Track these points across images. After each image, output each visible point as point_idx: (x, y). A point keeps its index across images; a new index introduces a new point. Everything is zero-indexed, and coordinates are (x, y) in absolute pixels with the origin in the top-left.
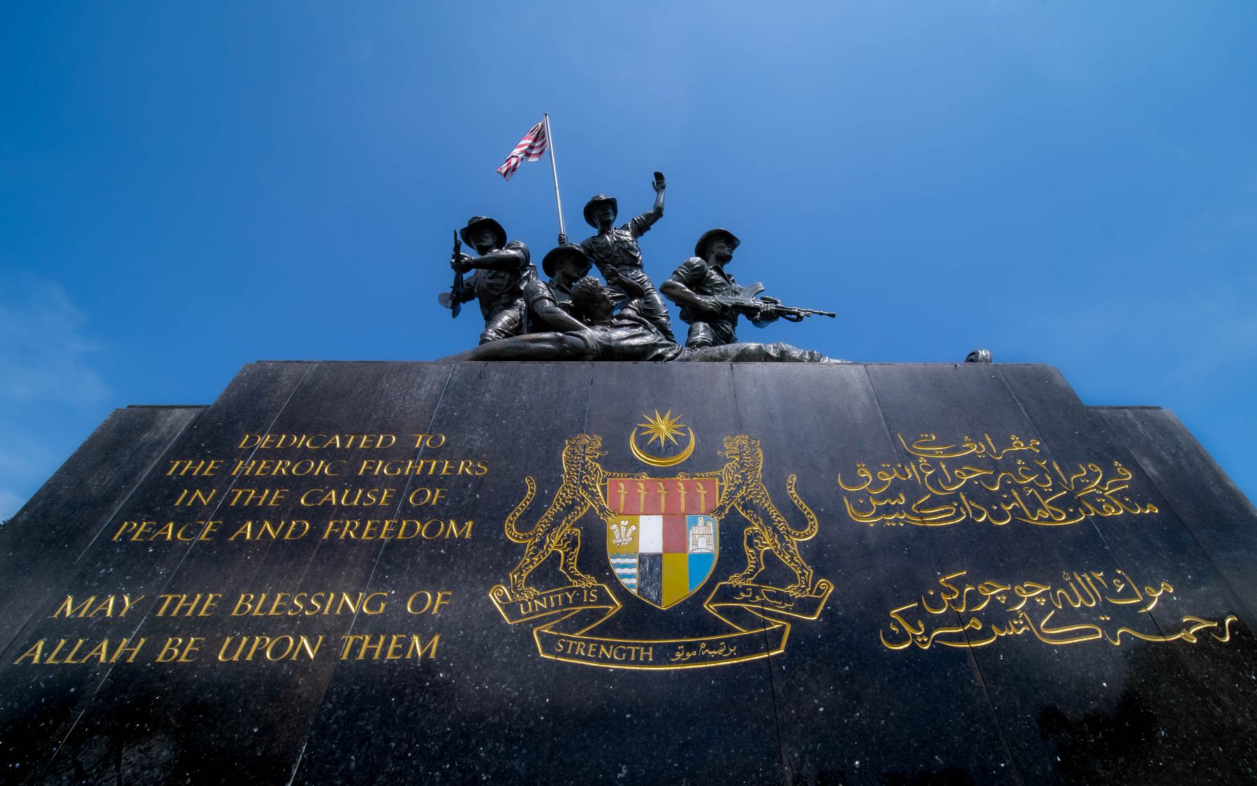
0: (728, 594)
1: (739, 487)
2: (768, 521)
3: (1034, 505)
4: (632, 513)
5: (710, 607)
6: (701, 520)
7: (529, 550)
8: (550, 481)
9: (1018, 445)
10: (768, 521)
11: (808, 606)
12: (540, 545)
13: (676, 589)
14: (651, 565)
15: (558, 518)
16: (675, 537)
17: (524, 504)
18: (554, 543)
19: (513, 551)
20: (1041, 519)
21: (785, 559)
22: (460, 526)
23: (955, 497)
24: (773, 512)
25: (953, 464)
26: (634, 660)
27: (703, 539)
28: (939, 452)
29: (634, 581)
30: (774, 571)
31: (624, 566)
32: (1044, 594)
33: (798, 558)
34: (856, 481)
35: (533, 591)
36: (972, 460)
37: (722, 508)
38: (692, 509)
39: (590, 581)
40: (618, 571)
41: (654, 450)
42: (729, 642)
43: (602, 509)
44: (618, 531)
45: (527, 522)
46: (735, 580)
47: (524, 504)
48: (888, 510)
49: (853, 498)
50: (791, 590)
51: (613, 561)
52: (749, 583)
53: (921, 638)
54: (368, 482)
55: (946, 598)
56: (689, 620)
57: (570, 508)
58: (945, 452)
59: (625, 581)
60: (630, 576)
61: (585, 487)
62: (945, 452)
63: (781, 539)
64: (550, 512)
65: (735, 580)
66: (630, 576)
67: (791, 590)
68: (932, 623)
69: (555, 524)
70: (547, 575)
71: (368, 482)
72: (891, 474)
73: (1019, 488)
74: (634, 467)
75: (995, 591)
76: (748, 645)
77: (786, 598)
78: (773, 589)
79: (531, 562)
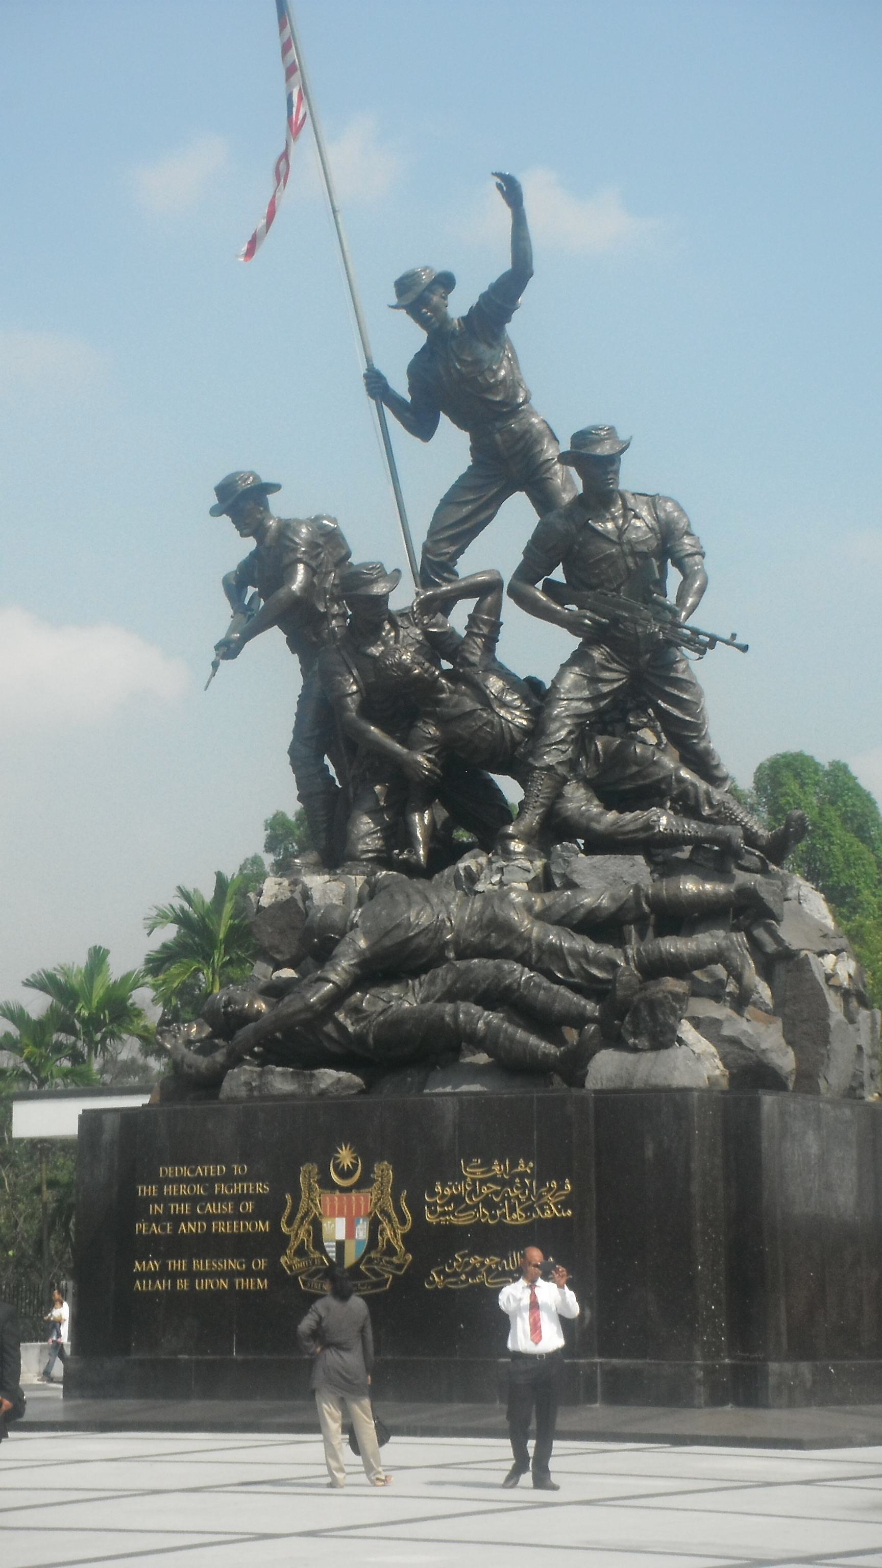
0: (370, 1261)
1: (379, 1200)
2: (390, 1221)
3: (512, 1210)
4: (333, 1216)
5: (362, 1267)
6: (361, 1221)
7: (292, 1237)
8: (297, 1199)
10: (390, 1221)
11: (399, 1267)
12: (297, 1234)
13: (350, 1259)
14: (340, 1245)
15: (303, 1218)
16: (350, 1231)
17: (287, 1211)
18: (302, 1234)
19: (288, 1238)
20: (512, 1220)
21: (394, 1242)
22: (264, 1224)
23: (477, 1206)
24: (394, 1214)
25: (483, 1182)
27: (362, 1232)
28: (479, 1174)
29: (334, 1254)
30: (390, 1250)
31: (329, 1246)
32: (497, 1264)
33: (400, 1243)
34: (433, 1194)
35: (297, 1259)
36: (494, 1180)
37: (371, 1213)
38: (358, 1214)
39: (317, 1255)
40: (327, 1249)
41: (345, 1174)
42: (369, 1284)
43: (320, 1214)
44: (326, 1225)
45: (289, 1223)
46: (373, 1255)
47: (287, 1211)
48: (444, 1213)
49: (429, 1205)
50: (394, 1259)
51: (325, 1244)
52: (378, 1255)
54: (221, 1198)
55: (455, 1264)
57: (306, 1214)
58: (482, 1173)
59: (330, 1254)
60: (332, 1252)
61: (312, 1201)
62: (482, 1173)
63: (394, 1232)
64: (299, 1216)
65: (373, 1255)
66: (332, 1252)
67: (394, 1259)
68: (447, 1276)
69: (301, 1223)
70: (301, 1252)
71: (221, 1198)
72: (451, 1188)
73: (509, 1198)
74: (333, 1187)
76: (375, 1285)
77: (392, 1263)
78: (388, 1259)
79: (294, 1244)
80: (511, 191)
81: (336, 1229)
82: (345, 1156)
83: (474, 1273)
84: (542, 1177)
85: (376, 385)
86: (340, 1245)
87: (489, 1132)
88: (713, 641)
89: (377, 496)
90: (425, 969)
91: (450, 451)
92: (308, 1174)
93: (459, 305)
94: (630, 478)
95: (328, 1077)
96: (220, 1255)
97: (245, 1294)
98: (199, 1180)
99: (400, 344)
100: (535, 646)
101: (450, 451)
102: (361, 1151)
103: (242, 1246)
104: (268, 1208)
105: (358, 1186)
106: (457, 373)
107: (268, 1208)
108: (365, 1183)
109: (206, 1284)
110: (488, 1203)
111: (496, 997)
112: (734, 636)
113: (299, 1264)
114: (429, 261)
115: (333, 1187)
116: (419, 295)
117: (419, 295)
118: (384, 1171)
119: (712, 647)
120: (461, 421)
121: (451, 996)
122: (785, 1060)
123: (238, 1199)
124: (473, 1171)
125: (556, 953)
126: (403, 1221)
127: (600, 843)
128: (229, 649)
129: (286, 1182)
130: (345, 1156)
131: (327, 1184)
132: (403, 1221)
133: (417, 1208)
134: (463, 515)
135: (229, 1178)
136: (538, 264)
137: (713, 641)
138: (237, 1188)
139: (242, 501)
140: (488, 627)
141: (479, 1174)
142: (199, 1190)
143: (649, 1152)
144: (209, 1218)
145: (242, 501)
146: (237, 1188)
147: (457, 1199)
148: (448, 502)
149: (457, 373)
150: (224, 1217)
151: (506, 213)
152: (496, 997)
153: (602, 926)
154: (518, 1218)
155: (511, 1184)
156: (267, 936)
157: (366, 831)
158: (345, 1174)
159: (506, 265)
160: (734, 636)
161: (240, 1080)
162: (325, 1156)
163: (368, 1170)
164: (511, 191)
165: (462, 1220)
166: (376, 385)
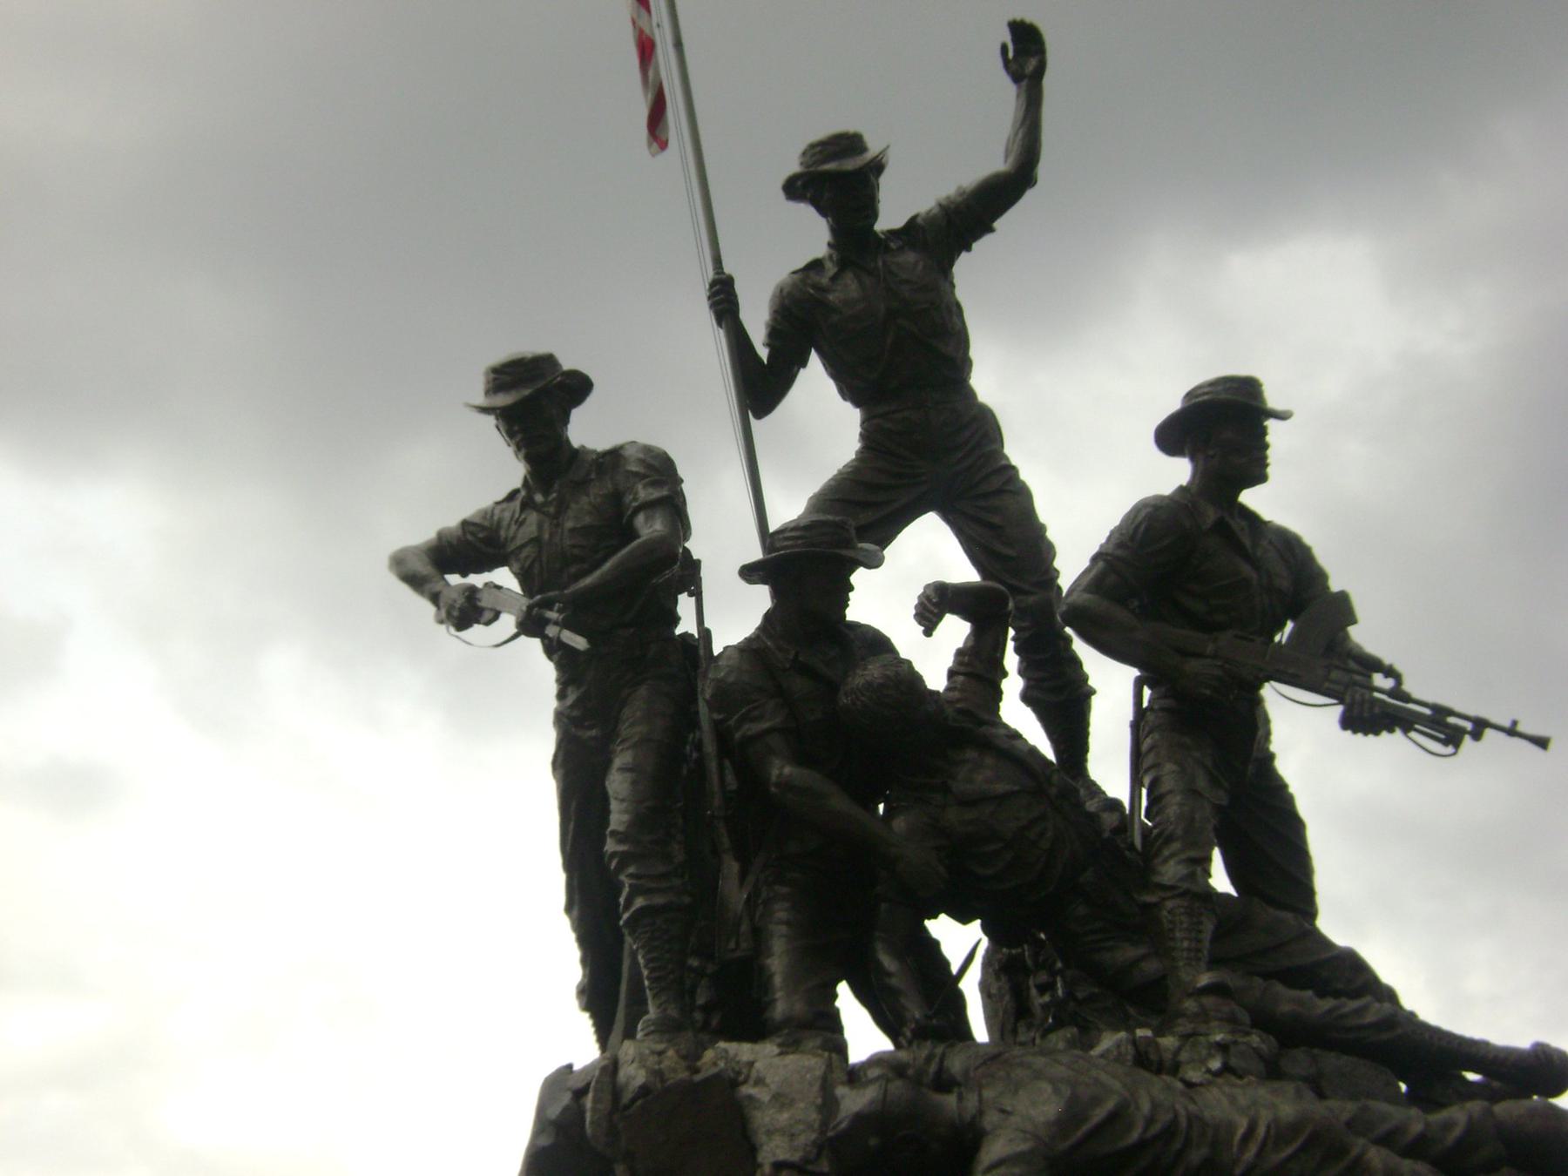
88: (1480, 726)
93: (895, 208)
101: (822, 427)
112: (1515, 723)
116: (836, 179)
117: (836, 179)
119: (1477, 735)
120: (852, 387)
136: (1043, 170)
137: (1480, 726)
139: (534, 398)
151: (1005, 95)
159: (994, 161)
160: (1515, 723)
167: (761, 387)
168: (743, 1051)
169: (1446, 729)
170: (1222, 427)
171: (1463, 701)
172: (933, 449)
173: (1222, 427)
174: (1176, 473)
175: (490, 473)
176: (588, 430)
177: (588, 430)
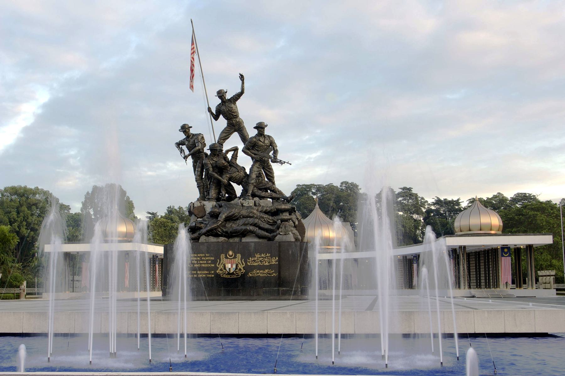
8: (220, 260)
9: (268, 255)
13: (231, 272)
14: (230, 269)
16: (232, 266)
18: (221, 267)
26: (229, 277)
27: (234, 266)
28: (259, 256)
30: (240, 270)
44: (227, 265)
53: (251, 275)
54: (203, 260)
56: (233, 274)
70: (221, 270)
71: (203, 260)
74: (228, 258)
75: (258, 271)
79: (220, 269)
80: (242, 77)
81: (229, 266)
82: (231, 253)
83: (258, 273)
84: (271, 257)
85: (209, 110)
86: (230, 269)
87: (258, 250)
88: (285, 162)
89: (210, 131)
90: (237, 219)
91: (222, 122)
92: (223, 256)
93: (228, 96)
94: (267, 132)
95: (222, 239)
96: (203, 270)
97: (208, 277)
98: (198, 257)
99: (215, 102)
100: (245, 162)
101: (222, 122)
102: (234, 252)
103: (208, 269)
104: (214, 262)
105: (233, 258)
106: (226, 109)
107: (214, 262)
108: (235, 257)
109: (200, 276)
110: (261, 261)
111: (255, 225)
113: (221, 272)
114: (224, 88)
115: (228, 258)
116: (221, 94)
117: (221, 94)
118: (239, 256)
120: (226, 117)
121: (245, 224)
122: (300, 237)
123: (207, 260)
124: (258, 256)
125: (263, 218)
126: (243, 264)
127: (261, 198)
128: (185, 158)
129: (218, 257)
130: (231, 253)
131: (226, 258)
132: (243, 264)
133: (246, 262)
134: (225, 135)
135: (205, 257)
136: (245, 91)
138: (207, 258)
139: (185, 129)
140: (235, 156)
141: (259, 256)
142: (199, 259)
143: (290, 253)
144: (201, 264)
145: (185, 129)
146: (207, 258)
147: (254, 261)
148: (223, 132)
149: (226, 109)
150: (205, 264)
151: (241, 82)
152: (255, 225)
153: (266, 212)
154: (267, 264)
155: (265, 258)
156: (196, 212)
157: (213, 193)
158: (232, 256)
159: (240, 91)
161: (203, 239)
162: (226, 253)
163: (235, 255)
164: (242, 77)
165: (256, 264)
166: (209, 110)
167: (216, 117)
168: (205, 203)
169: (282, 163)
170: (260, 127)
171: (283, 160)
172: (235, 125)
173: (260, 127)
174: (256, 132)
175: (182, 136)
176: (192, 131)
177: (192, 131)
